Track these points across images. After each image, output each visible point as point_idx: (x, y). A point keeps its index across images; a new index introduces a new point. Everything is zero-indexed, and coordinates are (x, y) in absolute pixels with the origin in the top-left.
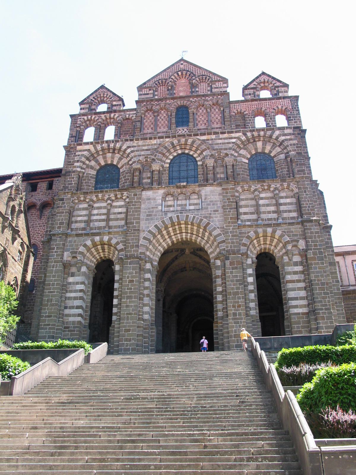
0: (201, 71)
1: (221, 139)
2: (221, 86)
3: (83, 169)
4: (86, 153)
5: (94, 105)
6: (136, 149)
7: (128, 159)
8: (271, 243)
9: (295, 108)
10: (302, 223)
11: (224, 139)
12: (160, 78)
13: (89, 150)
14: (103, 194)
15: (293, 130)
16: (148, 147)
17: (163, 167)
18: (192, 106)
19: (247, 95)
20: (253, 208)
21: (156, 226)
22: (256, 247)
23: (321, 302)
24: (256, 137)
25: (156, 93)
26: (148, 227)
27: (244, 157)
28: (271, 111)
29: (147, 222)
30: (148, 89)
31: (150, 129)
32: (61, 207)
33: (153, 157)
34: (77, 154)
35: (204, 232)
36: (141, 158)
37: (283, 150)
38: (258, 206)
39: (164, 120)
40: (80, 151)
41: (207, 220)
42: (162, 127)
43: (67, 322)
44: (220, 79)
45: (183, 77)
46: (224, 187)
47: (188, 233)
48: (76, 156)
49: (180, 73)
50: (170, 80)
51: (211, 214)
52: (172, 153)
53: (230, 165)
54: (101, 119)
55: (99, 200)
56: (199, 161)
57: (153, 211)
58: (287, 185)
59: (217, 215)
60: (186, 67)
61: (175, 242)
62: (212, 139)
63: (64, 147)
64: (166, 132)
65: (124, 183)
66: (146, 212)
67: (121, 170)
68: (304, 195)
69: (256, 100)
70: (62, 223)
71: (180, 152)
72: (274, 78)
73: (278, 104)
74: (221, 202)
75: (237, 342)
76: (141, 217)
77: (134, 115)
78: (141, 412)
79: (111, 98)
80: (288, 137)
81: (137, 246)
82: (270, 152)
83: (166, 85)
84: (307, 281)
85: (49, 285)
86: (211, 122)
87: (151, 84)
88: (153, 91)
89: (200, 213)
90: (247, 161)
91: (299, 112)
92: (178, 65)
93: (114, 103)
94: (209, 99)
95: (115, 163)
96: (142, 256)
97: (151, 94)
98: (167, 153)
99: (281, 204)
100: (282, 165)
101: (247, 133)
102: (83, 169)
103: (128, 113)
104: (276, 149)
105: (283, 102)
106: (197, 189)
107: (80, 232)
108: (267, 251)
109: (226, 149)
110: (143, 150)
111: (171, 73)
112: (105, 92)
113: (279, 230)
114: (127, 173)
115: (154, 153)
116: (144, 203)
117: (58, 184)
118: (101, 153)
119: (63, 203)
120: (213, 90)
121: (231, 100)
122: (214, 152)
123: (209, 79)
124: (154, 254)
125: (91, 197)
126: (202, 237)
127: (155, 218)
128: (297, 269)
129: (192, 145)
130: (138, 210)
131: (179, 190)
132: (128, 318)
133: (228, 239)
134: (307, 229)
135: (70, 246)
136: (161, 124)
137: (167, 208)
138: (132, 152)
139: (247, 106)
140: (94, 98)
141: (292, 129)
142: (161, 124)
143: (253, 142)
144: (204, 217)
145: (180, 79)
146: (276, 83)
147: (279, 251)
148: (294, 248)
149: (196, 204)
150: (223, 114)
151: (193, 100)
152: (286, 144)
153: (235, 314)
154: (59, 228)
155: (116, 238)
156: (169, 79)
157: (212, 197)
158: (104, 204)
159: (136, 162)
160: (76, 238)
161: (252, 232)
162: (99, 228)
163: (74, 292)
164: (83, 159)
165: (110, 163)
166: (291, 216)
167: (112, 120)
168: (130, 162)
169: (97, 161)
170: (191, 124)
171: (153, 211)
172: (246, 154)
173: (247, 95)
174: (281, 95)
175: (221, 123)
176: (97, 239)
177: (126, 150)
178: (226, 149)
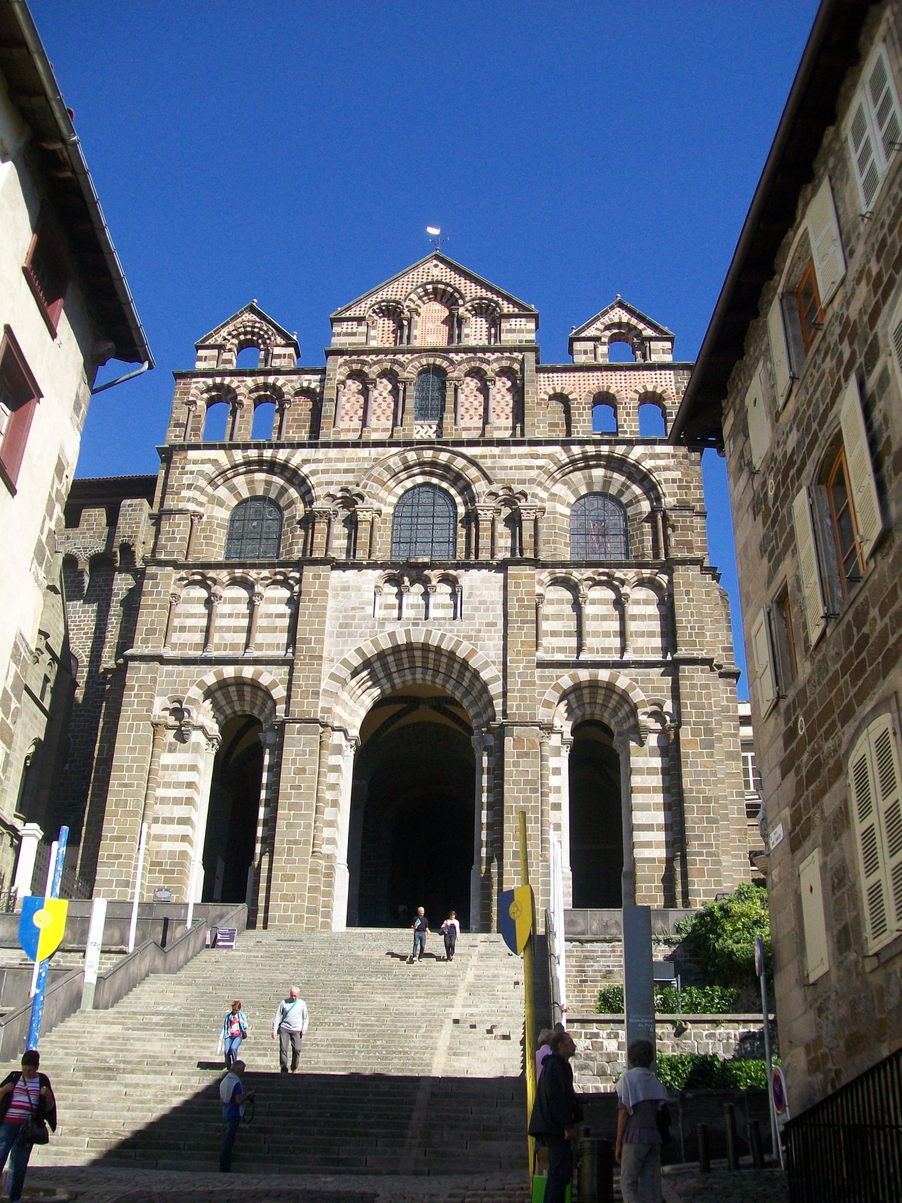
1: (513, 457)
2: (523, 327)
3: (201, 504)
4: (209, 469)
6: (321, 466)
11: (521, 457)
13: (215, 462)
14: (246, 571)
17: (379, 512)
21: (359, 651)
23: (700, 837)
25: (373, 333)
26: (342, 652)
27: (561, 501)
30: (355, 323)
32: (151, 593)
33: (359, 490)
34: (189, 468)
35: (463, 670)
36: (333, 490)
40: (195, 462)
43: (157, 852)
49: (430, 287)
50: (407, 303)
51: (479, 631)
54: (246, 386)
59: (493, 634)
60: (444, 274)
61: (399, 686)
62: (494, 457)
66: (338, 618)
67: (286, 514)
68: (683, 600)
71: (420, 479)
76: (328, 628)
80: (661, 463)
82: (621, 493)
85: (121, 769)
87: (362, 309)
90: (567, 511)
93: (277, 351)
97: (361, 334)
98: (391, 481)
101: (572, 447)
102: (201, 504)
110: (338, 471)
111: (410, 287)
113: (625, 675)
115: (362, 479)
116: (336, 596)
117: (130, 515)
119: (156, 586)
120: (504, 336)
125: (218, 575)
130: (321, 614)
131: (414, 573)
132: (290, 849)
138: (314, 473)
140: (229, 334)
155: (271, 673)
156: (405, 301)
157: (485, 592)
160: (181, 668)
164: (202, 483)
169: (233, 489)
170: (448, 417)
171: (354, 616)
172: (567, 495)
173: (579, 353)
176: (229, 671)
178: (522, 482)
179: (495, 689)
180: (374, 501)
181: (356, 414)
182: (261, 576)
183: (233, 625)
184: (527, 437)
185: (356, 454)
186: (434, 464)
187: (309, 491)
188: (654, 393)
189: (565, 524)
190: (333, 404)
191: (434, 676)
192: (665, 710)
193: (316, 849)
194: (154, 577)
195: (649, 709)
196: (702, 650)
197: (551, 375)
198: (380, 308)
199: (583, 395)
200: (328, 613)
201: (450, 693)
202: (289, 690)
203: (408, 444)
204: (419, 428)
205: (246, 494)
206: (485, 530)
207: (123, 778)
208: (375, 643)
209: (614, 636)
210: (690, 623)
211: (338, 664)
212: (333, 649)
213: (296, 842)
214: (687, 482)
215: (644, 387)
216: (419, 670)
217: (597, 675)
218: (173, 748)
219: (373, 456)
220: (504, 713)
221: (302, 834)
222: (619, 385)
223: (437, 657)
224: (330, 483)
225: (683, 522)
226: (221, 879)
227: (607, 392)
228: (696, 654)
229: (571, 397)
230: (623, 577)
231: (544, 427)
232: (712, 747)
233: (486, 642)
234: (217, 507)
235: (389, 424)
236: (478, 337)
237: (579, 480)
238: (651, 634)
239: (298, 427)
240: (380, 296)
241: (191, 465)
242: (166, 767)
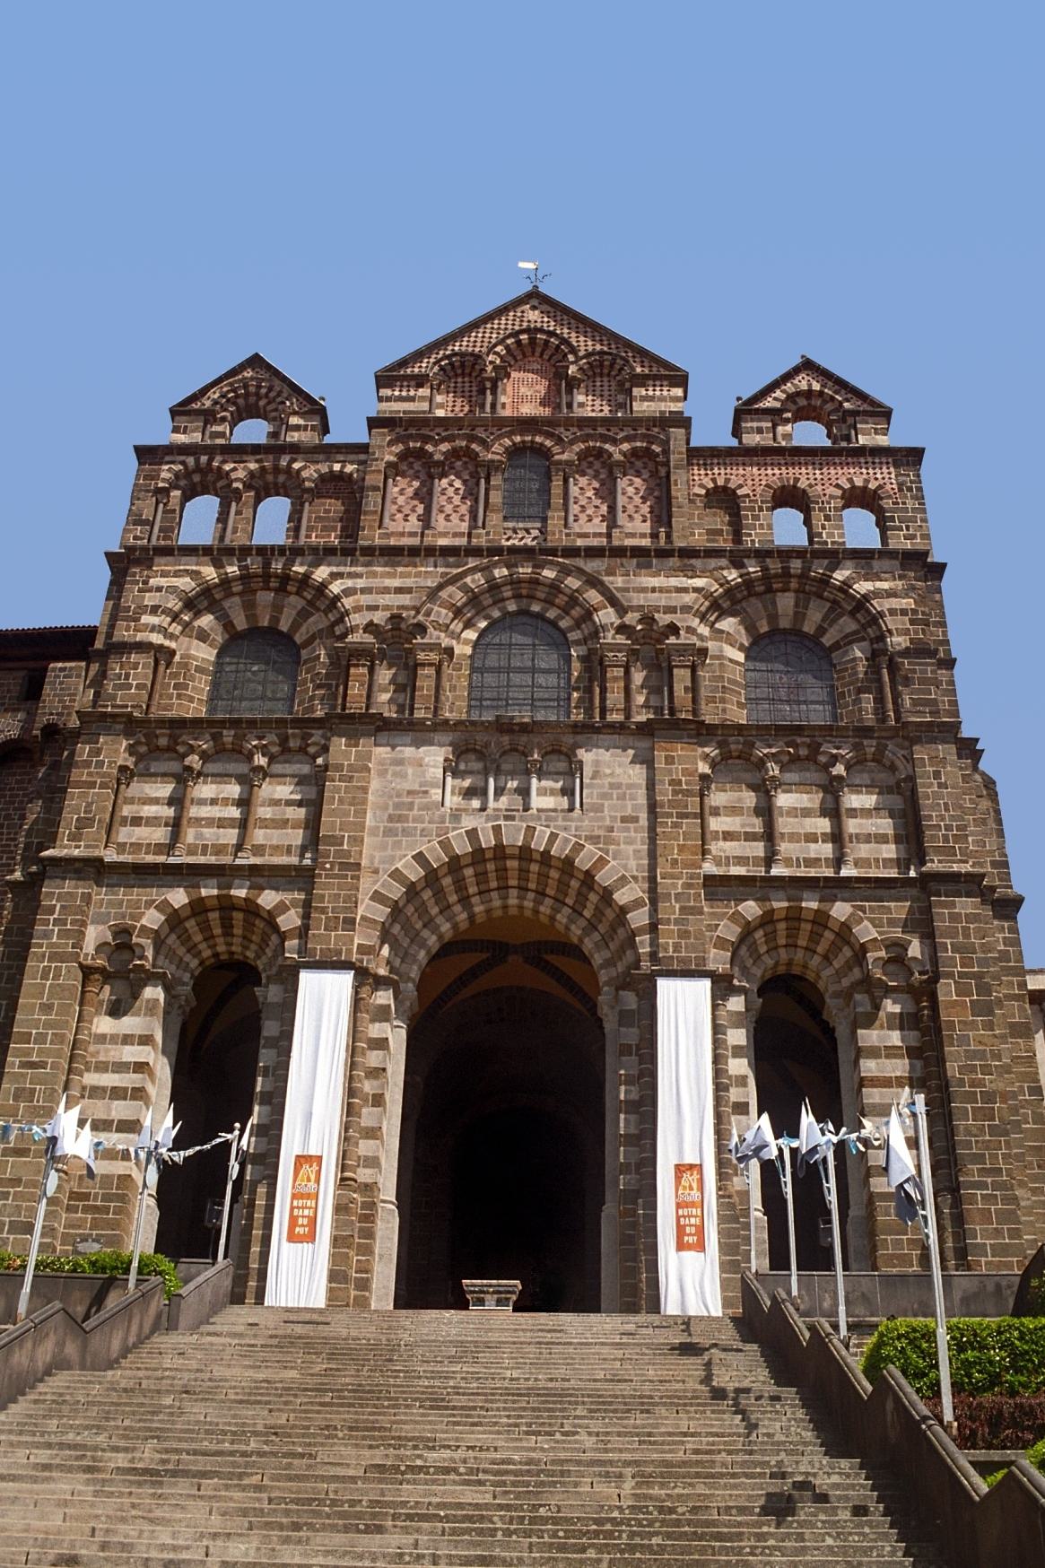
3: (172, 637)
4: (185, 583)
6: (360, 583)
7: (330, 615)
8: (812, 946)
9: (910, 489)
14: (240, 732)
17: (449, 652)
21: (420, 858)
22: (759, 956)
23: (979, 1158)
24: (776, 576)
28: (827, 492)
29: (390, 840)
32: (87, 764)
35: (584, 890)
36: (379, 617)
37: (864, 627)
41: (599, 849)
47: (527, 890)
48: (150, 590)
50: (491, 357)
51: (611, 829)
52: (484, 609)
55: (225, 750)
56: (577, 643)
57: (411, 806)
58: (877, 749)
59: (633, 834)
63: (108, 555)
68: (931, 785)
71: (512, 607)
72: (841, 384)
76: (369, 820)
78: (447, 1519)
81: (350, 923)
82: (821, 630)
83: (474, 374)
84: (933, 1083)
85: (26, 1038)
89: (573, 824)
90: (740, 657)
93: (294, 420)
95: (284, 626)
96: (365, 958)
97: (422, 398)
107: (150, 858)
108: (796, 971)
110: (386, 590)
111: (494, 336)
115: (424, 603)
116: (382, 773)
117: (61, 683)
118: (237, 588)
121: (692, 444)
123: (621, 369)
124: (406, 953)
126: (576, 907)
131: (506, 739)
133: (668, 922)
136: (451, 506)
138: (348, 592)
141: (896, 558)
142: (451, 506)
143: (765, 592)
144: (587, 838)
147: (839, 974)
150: (664, 490)
163: (113, 1072)
164: (174, 604)
165: (266, 624)
166: (885, 856)
167: (282, 478)
168: (336, 628)
170: (555, 518)
179: (639, 918)
180: (443, 635)
183: (218, 815)
184: (679, 543)
186: (535, 582)
187: (341, 620)
188: (865, 488)
189: (737, 674)
190: (380, 494)
191: (538, 902)
192: (910, 954)
193: (347, 1174)
198: (451, 364)
199: (759, 490)
200: (370, 797)
201: (561, 928)
202: (306, 916)
204: (510, 533)
206: (616, 679)
208: (445, 845)
209: (823, 841)
212: (377, 855)
214: (923, 613)
215: (850, 480)
216: (514, 893)
220: (653, 956)
224: (375, 608)
227: (795, 486)
229: (739, 492)
231: (700, 535)
232: (991, 1013)
233: (622, 846)
235: (464, 527)
238: (881, 839)
239: (324, 529)
242: (102, 1038)
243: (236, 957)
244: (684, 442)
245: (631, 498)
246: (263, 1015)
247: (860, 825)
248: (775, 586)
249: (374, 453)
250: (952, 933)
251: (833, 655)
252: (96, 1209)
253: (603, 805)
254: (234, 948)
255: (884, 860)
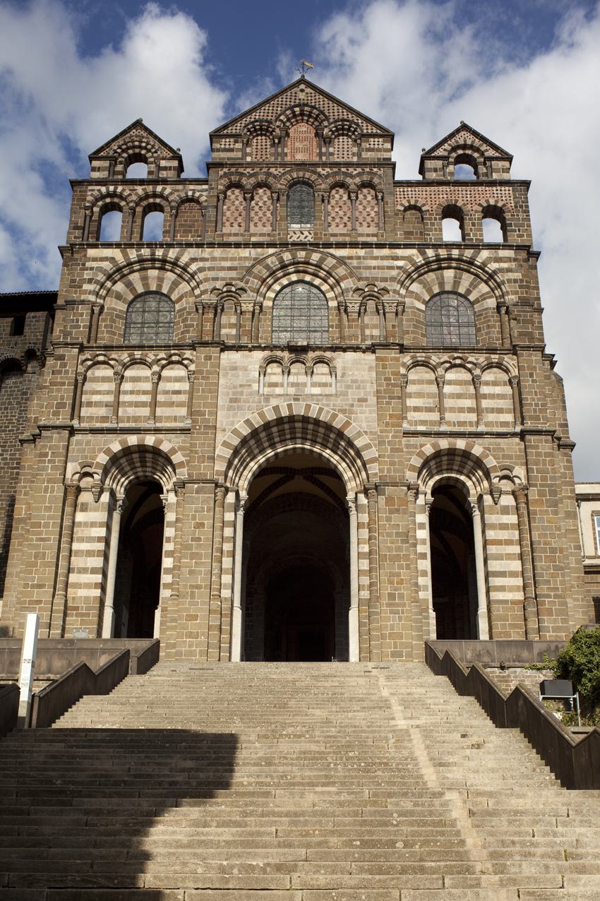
0: (340, 111)
1: (376, 258)
2: (380, 146)
4: (107, 265)
5: (121, 163)
6: (208, 264)
8: (461, 469)
9: (521, 207)
10: (522, 435)
11: (383, 258)
12: (257, 117)
13: (112, 260)
14: (144, 352)
15: (515, 253)
16: (233, 264)
18: (321, 184)
19: (430, 170)
20: (431, 400)
21: (248, 422)
23: (548, 582)
24: (444, 259)
25: (248, 150)
28: (474, 208)
29: (231, 413)
30: (232, 140)
31: (236, 225)
32: (60, 372)
33: (242, 284)
34: (88, 264)
36: (219, 285)
38: (441, 396)
39: (264, 209)
40: (95, 259)
42: (260, 224)
43: (73, 598)
44: (379, 131)
45: (302, 120)
46: (380, 353)
48: (87, 269)
50: (278, 123)
53: (393, 312)
54: (136, 194)
56: (332, 299)
59: (364, 408)
60: (310, 98)
62: (359, 258)
64: (269, 235)
65: (182, 333)
66: (228, 394)
68: (528, 381)
69: (447, 183)
70: (61, 405)
71: (294, 277)
72: (484, 140)
73: (488, 195)
74: (372, 383)
75: (395, 647)
77: (204, 193)
79: (156, 152)
80: (505, 265)
82: (469, 292)
86: (357, 221)
87: (238, 128)
88: (241, 144)
89: (332, 403)
90: (423, 307)
91: (529, 216)
92: (293, 91)
93: (163, 163)
94: (355, 172)
95: (165, 291)
96: (220, 478)
97: (238, 150)
99: (485, 396)
100: (489, 321)
101: (427, 250)
103: (192, 187)
104: (480, 286)
105: (499, 192)
106: (328, 354)
107: (98, 425)
109: (385, 280)
110: (223, 269)
111: (279, 109)
112: (143, 137)
114: (189, 313)
115: (244, 276)
116: (226, 375)
121: (397, 178)
122: (361, 283)
123: (355, 130)
127: (245, 406)
128: (506, 519)
129: (318, 266)
132: (193, 593)
134: (531, 447)
135: (79, 451)
137: (269, 389)
138: (201, 270)
139: (428, 193)
140: (120, 147)
142: (258, 217)
145: (298, 123)
146: (487, 151)
148: (504, 481)
149: (325, 385)
151: (324, 172)
152: (499, 278)
153: (392, 596)
154: (56, 414)
155: (171, 442)
156: (276, 122)
157: (356, 373)
158: (147, 372)
159: (209, 293)
160: (90, 437)
161: (428, 446)
162: (136, 419)
163: (86, 542)
164: (101, 277)
172: (422, 293)
173: (430, 170)
174: (495, 176)
175: (378, 225)
177: (187, 265)
178: (385, 280)
181: (236, 220)
182: (158, 358)
185: (239, 255)
188: (495, 206)
194: (61, 358)
195: (500, 474)
196: (546, 424)
197: (406, 189)
198: (254, 127)
199: (435, 207)
203: (284, 245)
205: (140, 290)
207: (40, 533)
208: (262, 415)
210: (533, 401)
211: (230, 433)
213: (198, 587)
217: (455, 444)
218: (84, 507)
219: (253, 255)
221: (203, 580)
222: (465, 199)
223: (316, 428)
225: (525, 316)
226: (126, 626)
227: (455, 205)
228: (540, 427)
229: (424, 209)
230: (475, 361)
231: (401, 234)
233: (359, 415)
234: (114, 300)
236: (341, 156)
237: (433, 280)
240: (253, 117)
241: (90, 263)
243: (148, 478)
244: (392, 178)
245: (361, 212)
246: (166, 510)
247: (489, 403)
248: (443, 265)
249: (211, 185)
250: (537, 463)
251: (475, 306)
252: (82, 615)
253: (348, 392)
254: (147, 474)
255: (501, 422)
